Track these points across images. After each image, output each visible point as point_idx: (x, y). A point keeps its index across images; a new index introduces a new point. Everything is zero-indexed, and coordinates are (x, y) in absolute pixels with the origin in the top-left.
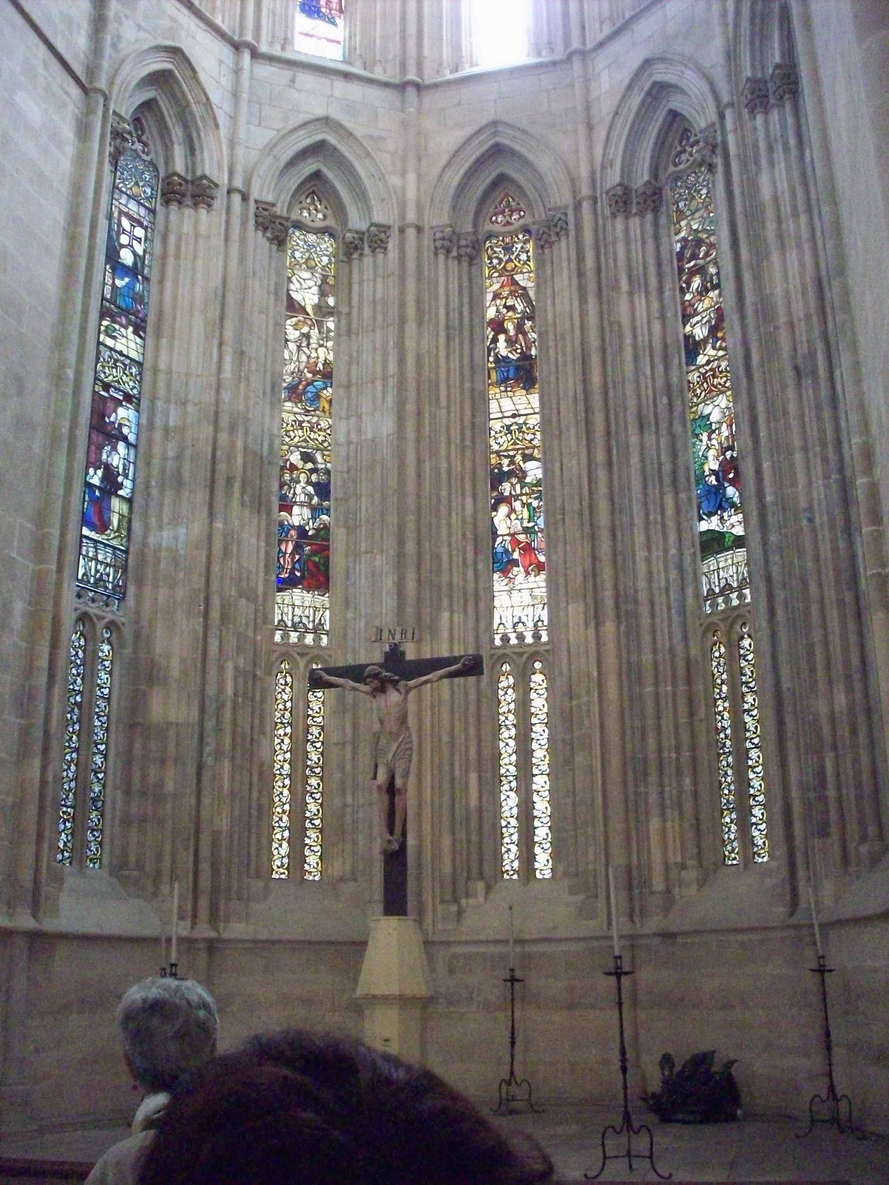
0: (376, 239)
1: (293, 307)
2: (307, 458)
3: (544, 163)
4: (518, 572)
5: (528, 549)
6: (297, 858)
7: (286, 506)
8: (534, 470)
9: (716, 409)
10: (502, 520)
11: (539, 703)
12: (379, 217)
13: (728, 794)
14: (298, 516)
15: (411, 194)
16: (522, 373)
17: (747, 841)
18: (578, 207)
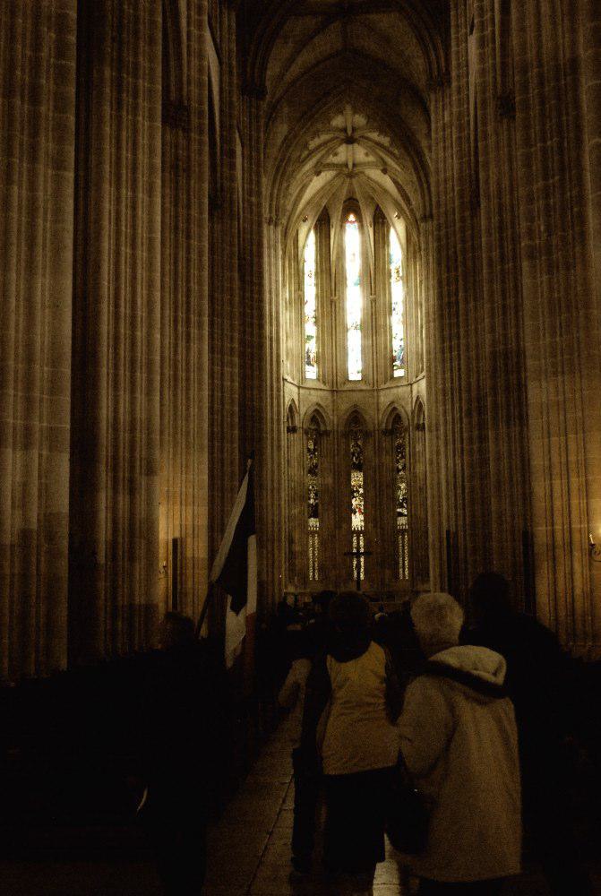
0: (327, 433)
1: (309, 450)
2: (313, 487)
3: (367, 417)
4: (357, 514)
5: (360, 509)
6: (314, 576)
7: (309, 499)
8: (361, 491)
9: (403, 486)
10: (354, 502)
11: (362, 543)
12: (328, 428)
13: (401, 565)
14: (312, 501)
15: (335, 422)
16: (359, 468)
17: (404, 574)
18: (374, 431)
